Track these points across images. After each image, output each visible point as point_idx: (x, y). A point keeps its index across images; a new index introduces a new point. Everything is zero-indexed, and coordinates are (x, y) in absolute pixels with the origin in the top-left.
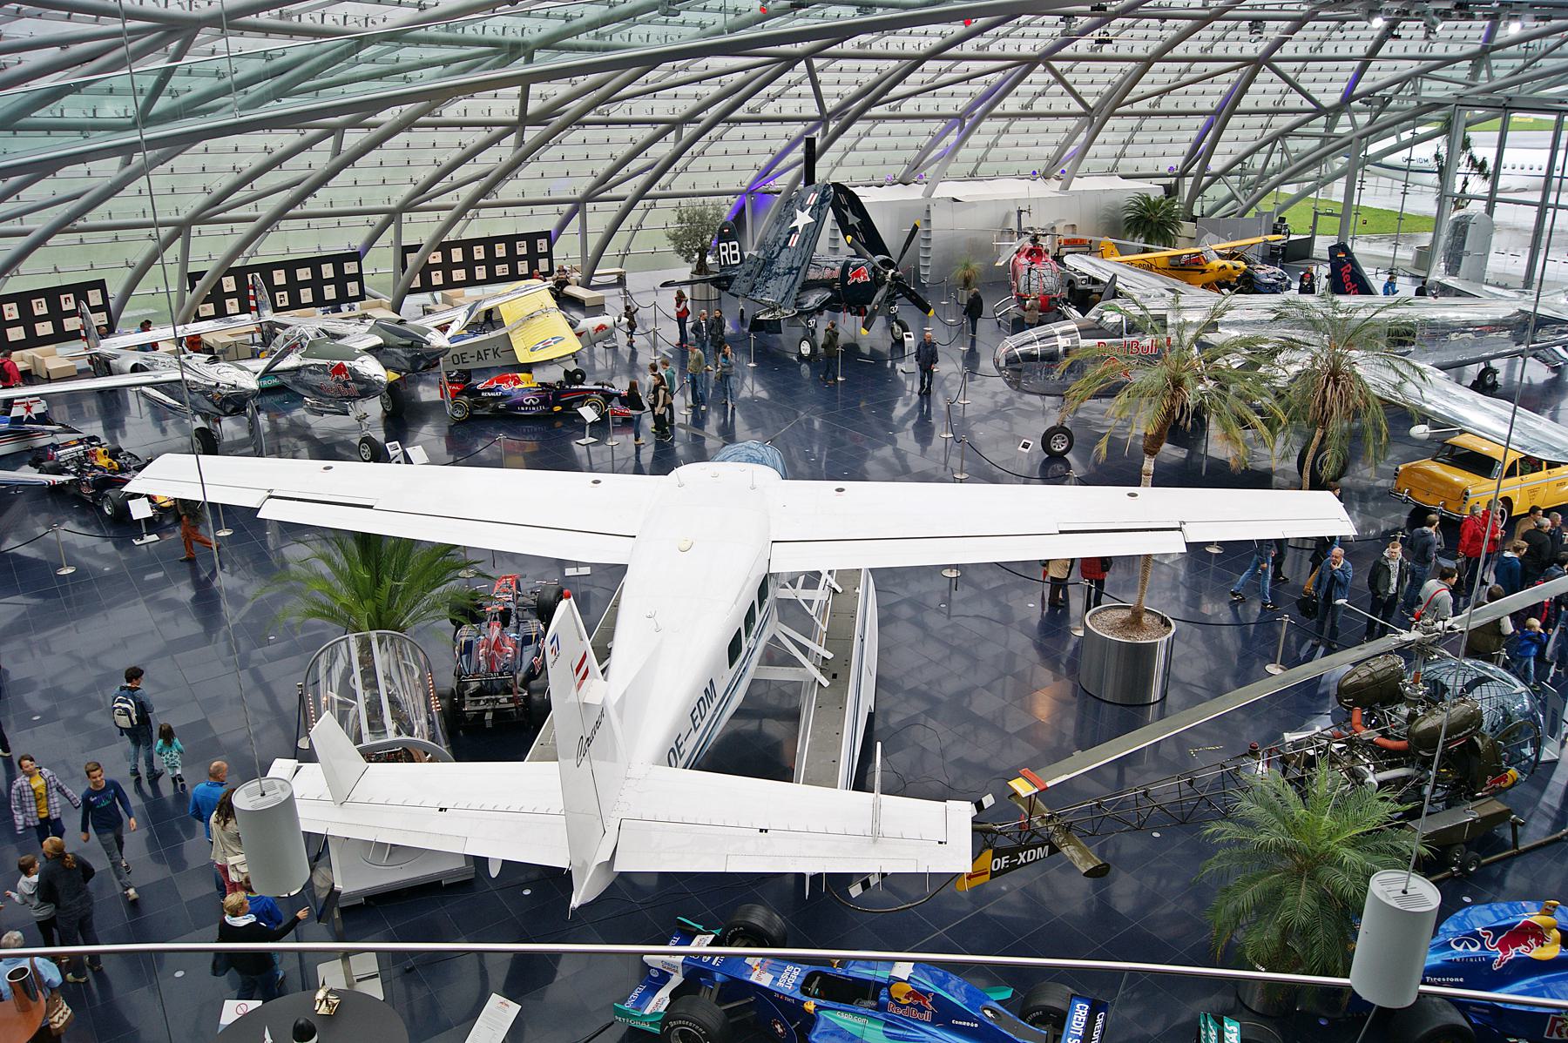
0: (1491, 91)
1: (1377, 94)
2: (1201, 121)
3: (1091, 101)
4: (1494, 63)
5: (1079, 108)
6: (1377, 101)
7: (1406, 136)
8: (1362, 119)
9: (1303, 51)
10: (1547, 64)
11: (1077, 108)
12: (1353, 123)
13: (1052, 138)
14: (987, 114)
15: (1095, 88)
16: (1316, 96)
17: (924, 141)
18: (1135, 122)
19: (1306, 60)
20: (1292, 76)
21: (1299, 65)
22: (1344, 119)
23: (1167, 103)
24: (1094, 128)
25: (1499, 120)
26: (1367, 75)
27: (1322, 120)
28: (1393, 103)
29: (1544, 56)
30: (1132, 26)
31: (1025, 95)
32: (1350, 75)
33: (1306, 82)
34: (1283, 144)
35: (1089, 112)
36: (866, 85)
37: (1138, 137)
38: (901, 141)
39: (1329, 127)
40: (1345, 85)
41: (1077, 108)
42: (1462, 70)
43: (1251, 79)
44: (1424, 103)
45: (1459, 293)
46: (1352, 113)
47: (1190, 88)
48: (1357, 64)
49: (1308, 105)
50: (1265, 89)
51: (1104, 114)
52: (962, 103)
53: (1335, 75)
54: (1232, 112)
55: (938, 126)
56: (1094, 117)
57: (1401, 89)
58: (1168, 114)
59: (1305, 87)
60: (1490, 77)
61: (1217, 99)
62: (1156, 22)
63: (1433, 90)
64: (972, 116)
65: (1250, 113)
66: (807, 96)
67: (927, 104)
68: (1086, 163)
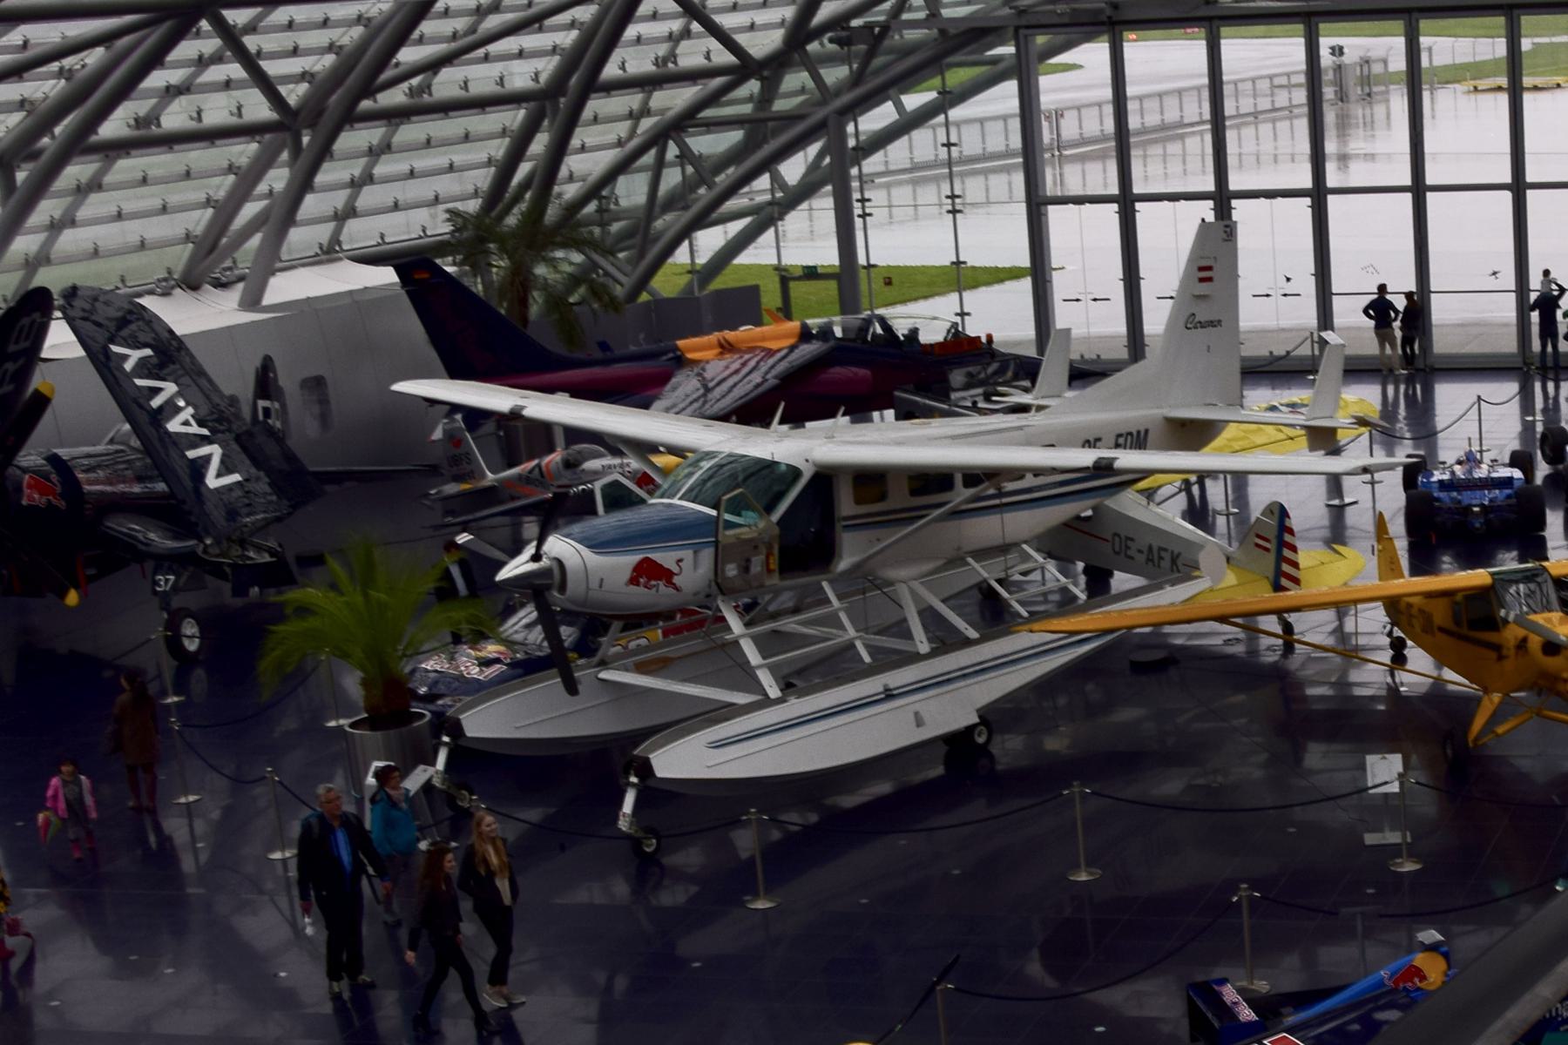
3: (294, 94)
11: (258, 109)
41: (258, 109)
45: (1040, 408)
51: (327, 121)
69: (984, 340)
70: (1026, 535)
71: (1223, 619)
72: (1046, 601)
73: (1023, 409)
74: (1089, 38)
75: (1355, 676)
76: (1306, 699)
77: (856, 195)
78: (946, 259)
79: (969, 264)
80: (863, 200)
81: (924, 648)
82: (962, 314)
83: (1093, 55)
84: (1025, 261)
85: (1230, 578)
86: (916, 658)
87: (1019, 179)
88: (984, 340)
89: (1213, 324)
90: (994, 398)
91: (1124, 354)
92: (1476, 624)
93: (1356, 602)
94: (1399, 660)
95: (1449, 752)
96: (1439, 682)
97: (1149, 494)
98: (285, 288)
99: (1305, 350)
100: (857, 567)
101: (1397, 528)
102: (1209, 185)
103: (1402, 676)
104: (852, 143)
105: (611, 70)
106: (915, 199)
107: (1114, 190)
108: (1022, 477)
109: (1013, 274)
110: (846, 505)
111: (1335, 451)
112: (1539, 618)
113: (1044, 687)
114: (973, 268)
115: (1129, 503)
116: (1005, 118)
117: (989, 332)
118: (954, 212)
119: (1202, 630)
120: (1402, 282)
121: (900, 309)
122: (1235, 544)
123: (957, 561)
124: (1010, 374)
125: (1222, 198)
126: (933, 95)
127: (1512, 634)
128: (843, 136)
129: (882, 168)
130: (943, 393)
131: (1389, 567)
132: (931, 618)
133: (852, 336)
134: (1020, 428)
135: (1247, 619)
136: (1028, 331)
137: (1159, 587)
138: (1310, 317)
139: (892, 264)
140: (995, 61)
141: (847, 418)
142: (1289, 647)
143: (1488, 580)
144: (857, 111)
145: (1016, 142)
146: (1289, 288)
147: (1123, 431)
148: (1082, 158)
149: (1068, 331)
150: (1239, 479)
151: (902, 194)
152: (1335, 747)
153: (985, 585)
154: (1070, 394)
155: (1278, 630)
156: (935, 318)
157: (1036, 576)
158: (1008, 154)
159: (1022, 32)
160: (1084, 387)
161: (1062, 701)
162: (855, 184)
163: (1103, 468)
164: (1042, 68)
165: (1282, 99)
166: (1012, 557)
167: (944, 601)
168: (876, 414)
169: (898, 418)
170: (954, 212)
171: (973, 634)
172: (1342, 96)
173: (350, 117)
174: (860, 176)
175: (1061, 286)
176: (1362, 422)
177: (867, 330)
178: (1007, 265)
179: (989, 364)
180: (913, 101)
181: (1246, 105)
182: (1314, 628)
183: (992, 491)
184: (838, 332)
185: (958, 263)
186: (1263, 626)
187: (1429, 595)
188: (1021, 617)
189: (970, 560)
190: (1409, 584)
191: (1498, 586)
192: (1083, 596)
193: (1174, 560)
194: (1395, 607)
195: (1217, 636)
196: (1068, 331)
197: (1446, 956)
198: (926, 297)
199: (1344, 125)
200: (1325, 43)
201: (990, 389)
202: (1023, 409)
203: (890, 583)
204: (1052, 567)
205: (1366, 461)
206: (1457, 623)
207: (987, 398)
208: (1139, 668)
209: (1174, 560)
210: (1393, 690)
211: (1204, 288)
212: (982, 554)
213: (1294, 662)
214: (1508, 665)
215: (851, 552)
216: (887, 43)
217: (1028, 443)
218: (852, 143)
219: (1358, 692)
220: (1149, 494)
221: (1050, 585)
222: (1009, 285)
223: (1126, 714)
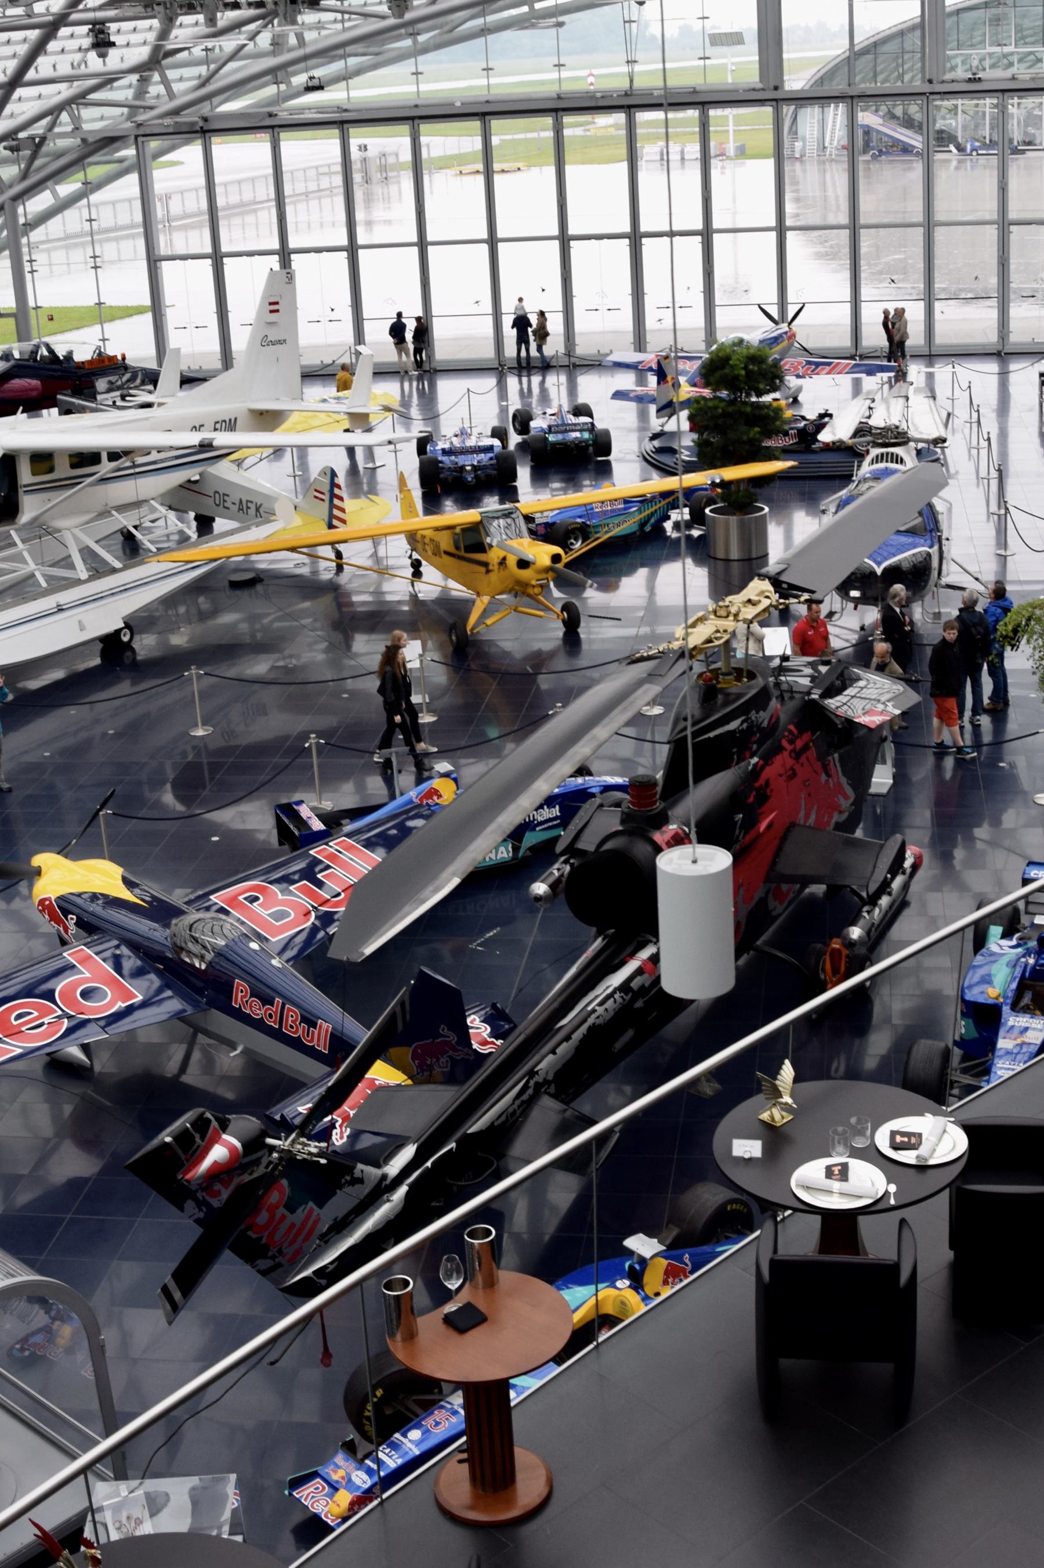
0: (176, 112)
1: (22, 135)
4: (171, 74)
10: (234, 71)
28: (50, 146)
29: (233, 56)
42: (123, 91)
44: (91, 140)
69: (119, 358)
70: (153, 493)
71: (293, 549)
72: (168, 540)
73: (148, 405)
74: (187, 142)
75: (387, 587)
76: (351, 604)
77: (26, 258)
78: (92, 301)
79: (108, 304)
80: (31, 261)
81: (84, 575)
82: (104, 340)
83: (191, 153)
84: (147, 302)
85: (297, 521)
86: (79, 582)
87: (141, 243)
88: (119, 358)
89: (279, 342)
90: (128, 398)
91: (218, 365)
92: (469, 549)
93: (386, 535)
94: (417, 574)
95: (454, 638)
96: (445, 589)
97: (239, 463)
99: (346, 360)
100: (35, 520)
101: (414, 483)
102: (275, 245)
103: (418, 586)
104: (22, 220)
106: (68, 258)
107: (209, 250)
108: (149, 453)
109: (139, 311)
110: (25, 475)
111: (369, 430)
112: (514, 543)
113: (170, 600)
114: (111, 307)
115: (224, 470)
116: (130, 201)
117: (123, 352)
118: (96, 267)
119: (279, 558)
120: (412, 311)
121: (59, 337)
122: (300, 497)
123: (104, 514)
124: (138, 381)
125: (285, 254)
126: (79, 185)
127: (494, 556)
128: (14, 216)
129: (44, 238)
130: (91, 394)
131: (408, 509)
132: (88, 554)
133: (26, 357)
134: (147, 419)
135: (310, 549)
136: (152, 351)
137: (248, 528)
138: (349, 337)
139: (53, 305)
140: (121, 161)
141: (25, 415)
142: (340, 568)
143: (478, 518)
144: (25, 198)
145: (138, 217)
146: (333, 316)
147: (220, 420)
148: (185, 228)
149: (179, 349)
150: (302, 451)
151: (59, 256)
152: (374, 637)
153: (125, 530)
154: (182, 394)
155: (333, 556)
156: (84, 343)
157: (161, 523)
158: (132, 226)
159: (140, 139)
160: (191, 389)
161: (182, 610)
162: (25, 250)
163: (206, 446)
164: (155, 164)
165: (325, 183)
166: (144, 510)
167: (97, 542)
168: (45, 412)
169: (60, 414)
170: (96, 267)
171: (118, 565)
172: (367, 180)
174: (29, 244)
175: (172, 318)
176: (387, 409)
177: (37, 353)
178: (135, 304)
179: (123, 375)
180: (66, 189)
181: (300, 188)
182: (356, 554)
183: (128, 464)
184: (17, 355)
185: (100, 304)
186: (321, 554)
187: (437, 529)
188: (151, 551)
189: (114, 512)
190: (424, 521)
191: (485, 522)
192: (194, 536)
193: (257, 510)
194: (413, 538)
195: (290, 563)
196: (179, 349)
197: (455, 780)
198: (78, 328)
199: (368, 200)
200: (354, 143)
201: (125, 392)
202: (148, 405)
203: (59, 531)
204: (172, 515)
205: (391, 436)
206: (457, 548)
207: (123, 398)
208: (235, 585)
209: (257, 510)
210: (414, 597)
211: (274, 317)
212: (122, 508)
213: (344, 579)
214: (494, 577)
215: (30, 507)
216: (44, 149)
217: (153, 429)
218: (22, 220)
219: (389, 598)
220: (239, 463)
221: (172, 529)
222: (136, 318)
223: (227, 618)
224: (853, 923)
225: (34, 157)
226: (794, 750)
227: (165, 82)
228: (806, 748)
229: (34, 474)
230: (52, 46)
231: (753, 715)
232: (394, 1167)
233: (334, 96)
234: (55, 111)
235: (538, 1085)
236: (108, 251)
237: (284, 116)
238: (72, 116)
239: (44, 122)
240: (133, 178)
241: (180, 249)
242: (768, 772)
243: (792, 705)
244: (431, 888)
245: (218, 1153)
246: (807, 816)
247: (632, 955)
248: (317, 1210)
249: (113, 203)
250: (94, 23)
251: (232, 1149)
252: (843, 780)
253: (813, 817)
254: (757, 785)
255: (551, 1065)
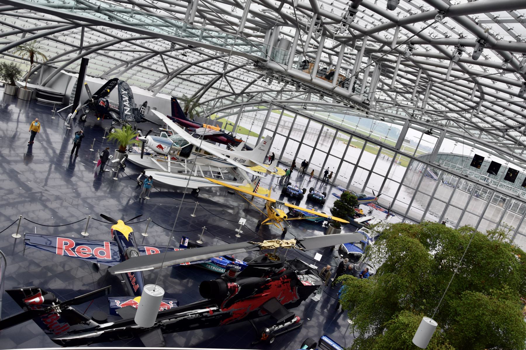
0: (281, 102)
1: (251, 94)
2: (200, 87)
3: (170, 71)
5: (166, 72)
6: (250, 96)
7: (255, 108)
8: (245, 100)
9: (235, 76)
10: (295, 99)
12: (242, 100)
13: (154, 78)
14: (137, 65)
15: (172, 67)
16: (234, 89)
17: (113, 66)
18: (181, 81)
19: (235, 78)
20: (230, 81)
21: (232, 79)
22: (240, 98)
23: (192, 78)
24: (169, 79)
25: (281, 111)
26: (250, 88)
27: (234, 97)
30: (190, 53)
31: (150, 62)
32: (245, 86)
33: (233, 85)
34: (222, 100)
35: (168, 74)
36: (99, 42)
37: (180, 86)
38: (105, 64)
39: (235, 99)
40: (243, 89)
42: (274, 94)
43: (218, 79)
46: (243, 97)
47: (200, 76)
48: (248, 84)
49: (231, 91)
50: (221, 84)
51: (173, 76)
52: (129, 58)
53: (241, 85)
54: (210, 87)
55: (119, 63)
56: (170, 76)
57: (257, 95)
58: (191, 81)
59: (232, 86)
60: (281, 99)
61: (207, 82)
62: (198, 54)
63: (265, 97)
64: (132, 63)
65: (215, 88)
66: (77, 39)
67: (118, 55)
68: (163, 89)
98: (159, 95)
105: (213, 86)
118: (252, 124)
145: (264, 119)
173: (175, 76)
224: (268, 328)
225: (250, 99)
226: (283, 281)
227: (281, 96)
228: (287, 282)
229: (196, 151)
230: (236, 71)
231: (273, 269)
232: (103, 326)
233: (312, 113)
234: (259, 92)
235: (160, 325)
236: (256, 122)
237: (300, 112)
238: (261, 94)
239: (256, 93)
240: (267, 111)
241: (269, 128)
242: (272, 283)
243: (288, 271)
244: (145, 267)
245: (37, 300)
246: (280, 298)
247: (209, 307)
248: (69, 325)
249: (261, 114)
250: (225, 63)
251: (41, 301)
252: (297, 294)
253: (283, 298)
254: (267, 284)
255: (166, 322)
